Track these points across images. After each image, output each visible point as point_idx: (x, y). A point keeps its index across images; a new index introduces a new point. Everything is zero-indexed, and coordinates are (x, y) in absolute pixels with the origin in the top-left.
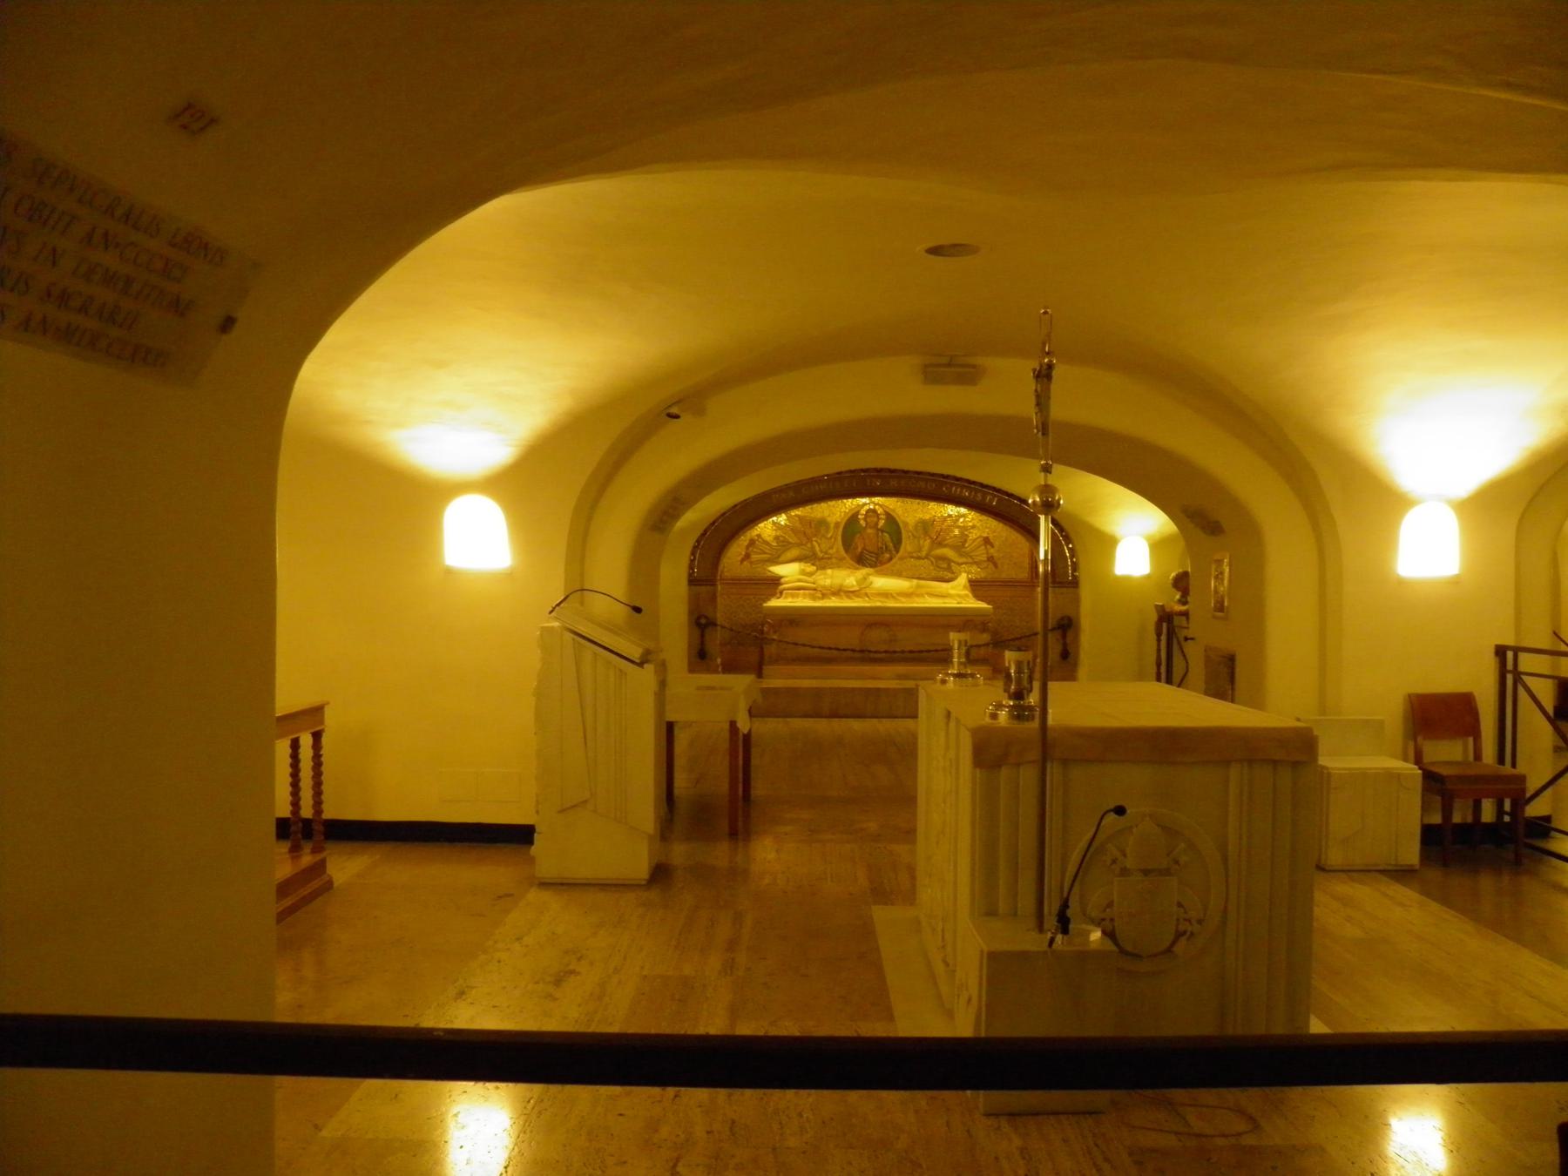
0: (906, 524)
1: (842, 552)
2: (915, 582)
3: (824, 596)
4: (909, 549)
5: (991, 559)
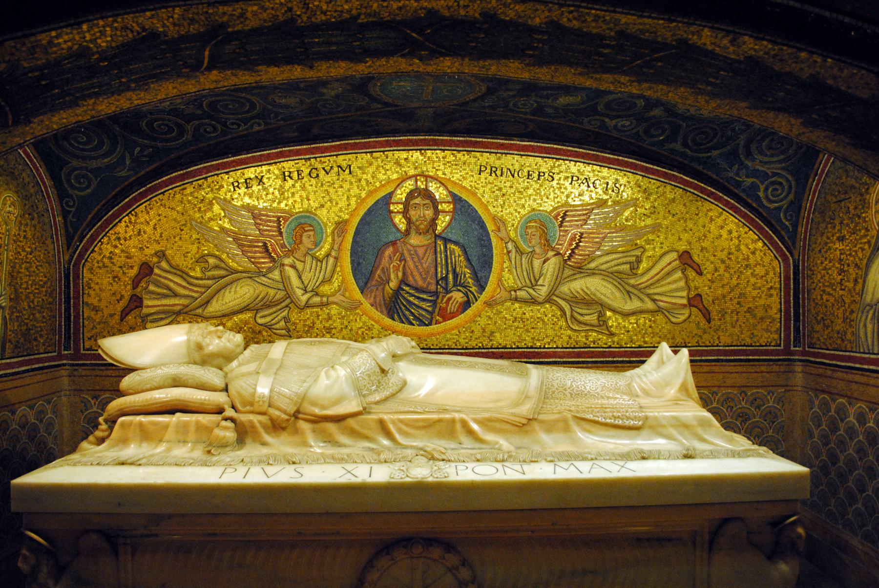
0: (500, 223)
1: (357, 294)
2: (535, 373)
3: (243, 434)
4: (509, 280)
5: (695, 301)
